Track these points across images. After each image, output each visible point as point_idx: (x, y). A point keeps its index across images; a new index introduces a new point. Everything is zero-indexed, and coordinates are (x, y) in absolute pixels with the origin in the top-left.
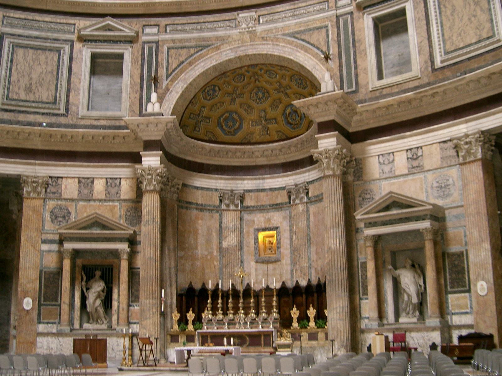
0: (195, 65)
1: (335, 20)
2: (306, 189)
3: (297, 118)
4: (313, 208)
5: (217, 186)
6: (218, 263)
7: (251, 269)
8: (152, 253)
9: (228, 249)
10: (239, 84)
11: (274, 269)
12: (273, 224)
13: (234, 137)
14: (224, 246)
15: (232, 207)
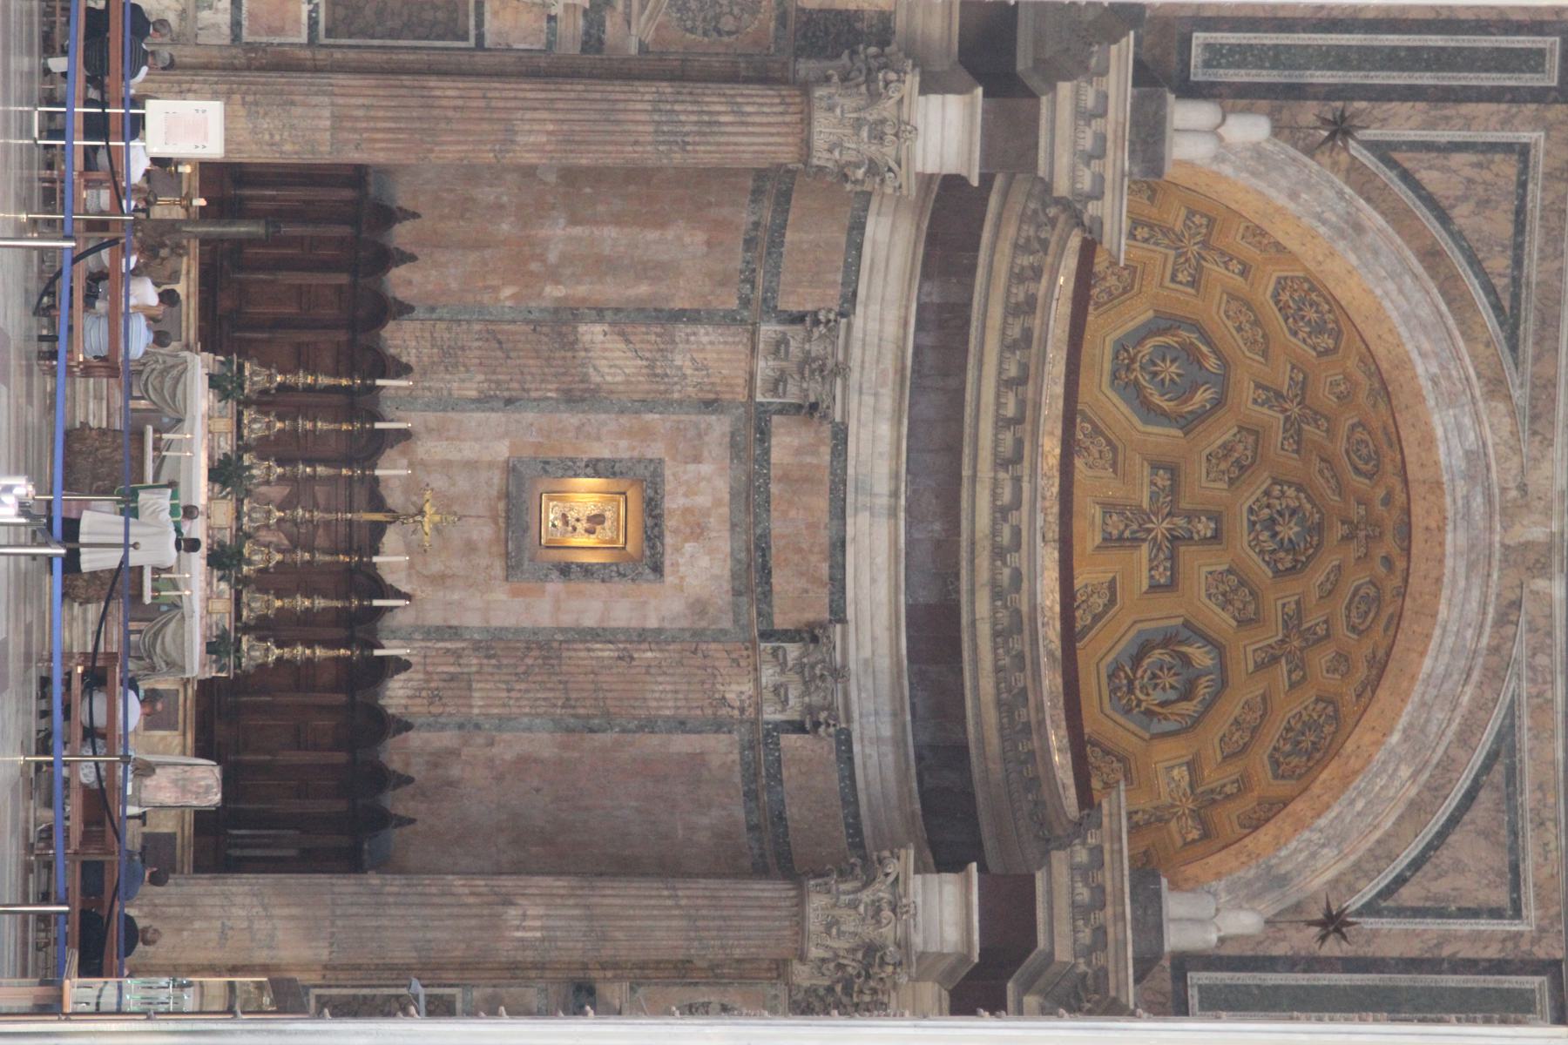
0: (1425, 276)
1: (1541, 953)
2: (817, 724)
3: (1157, 696)
4: (722, 749)
5: (866, 306)
6: (508, 303)
7: (477, 439)
8: (532, 139)
9: (572, 345)
10: (1342, 445)
11: (470, 548)
12: (678, 550)
13: (1106, 378)
14: (582, 328)
15: (765, 367)
